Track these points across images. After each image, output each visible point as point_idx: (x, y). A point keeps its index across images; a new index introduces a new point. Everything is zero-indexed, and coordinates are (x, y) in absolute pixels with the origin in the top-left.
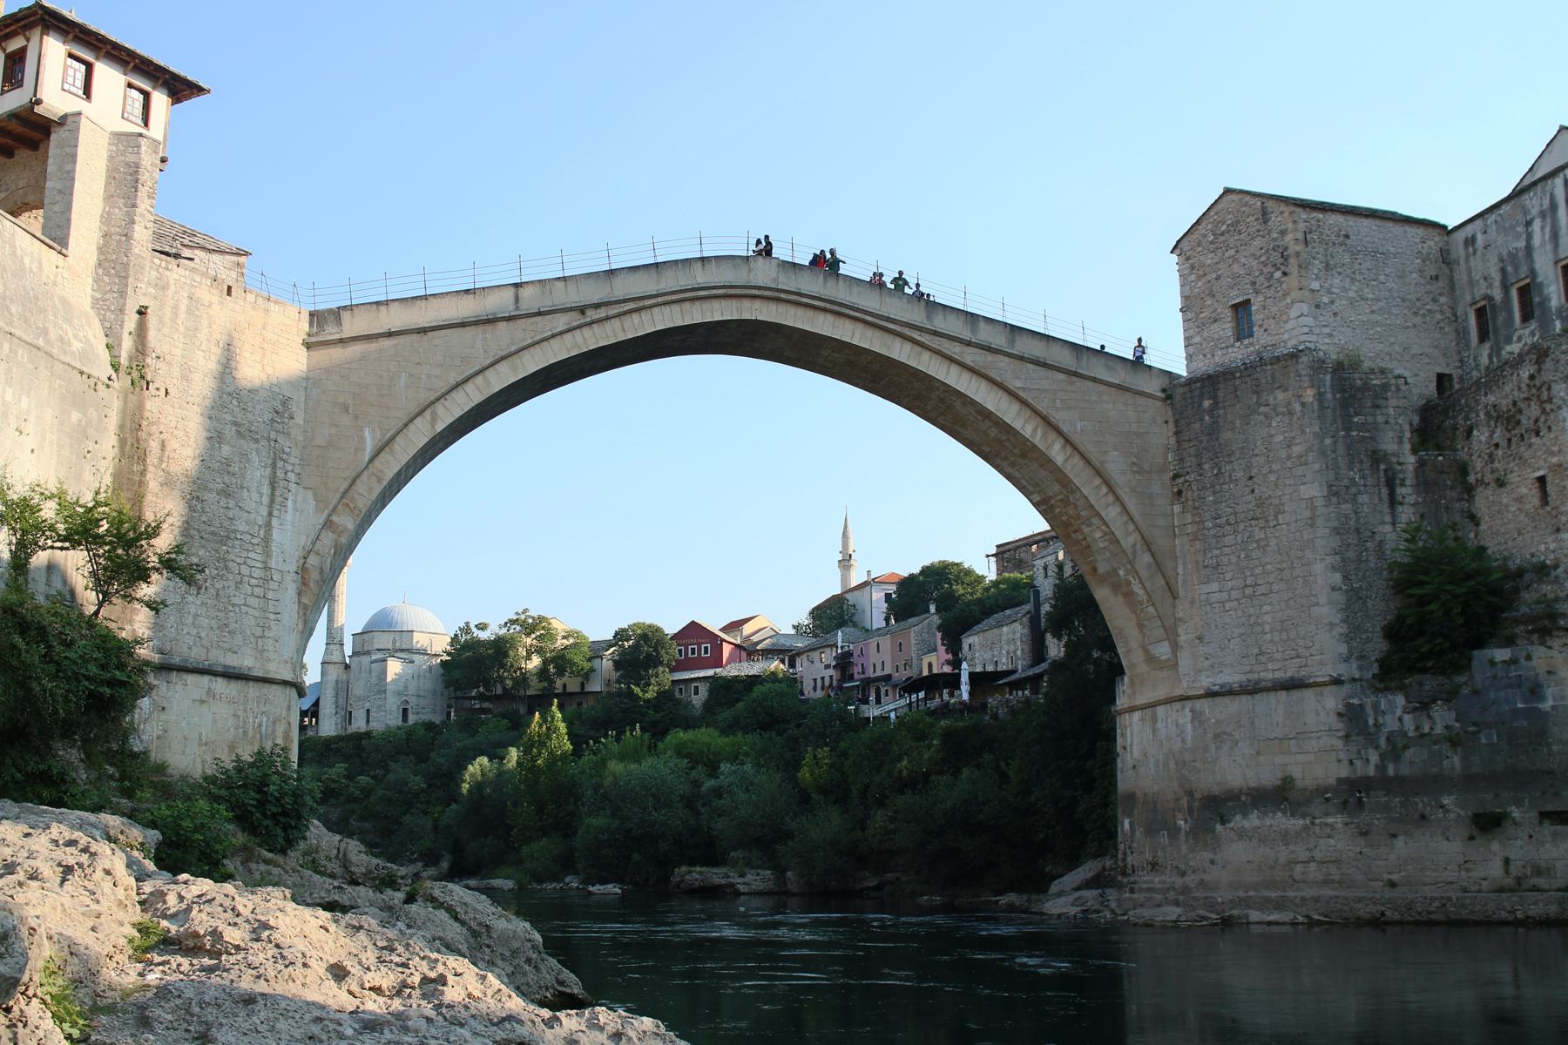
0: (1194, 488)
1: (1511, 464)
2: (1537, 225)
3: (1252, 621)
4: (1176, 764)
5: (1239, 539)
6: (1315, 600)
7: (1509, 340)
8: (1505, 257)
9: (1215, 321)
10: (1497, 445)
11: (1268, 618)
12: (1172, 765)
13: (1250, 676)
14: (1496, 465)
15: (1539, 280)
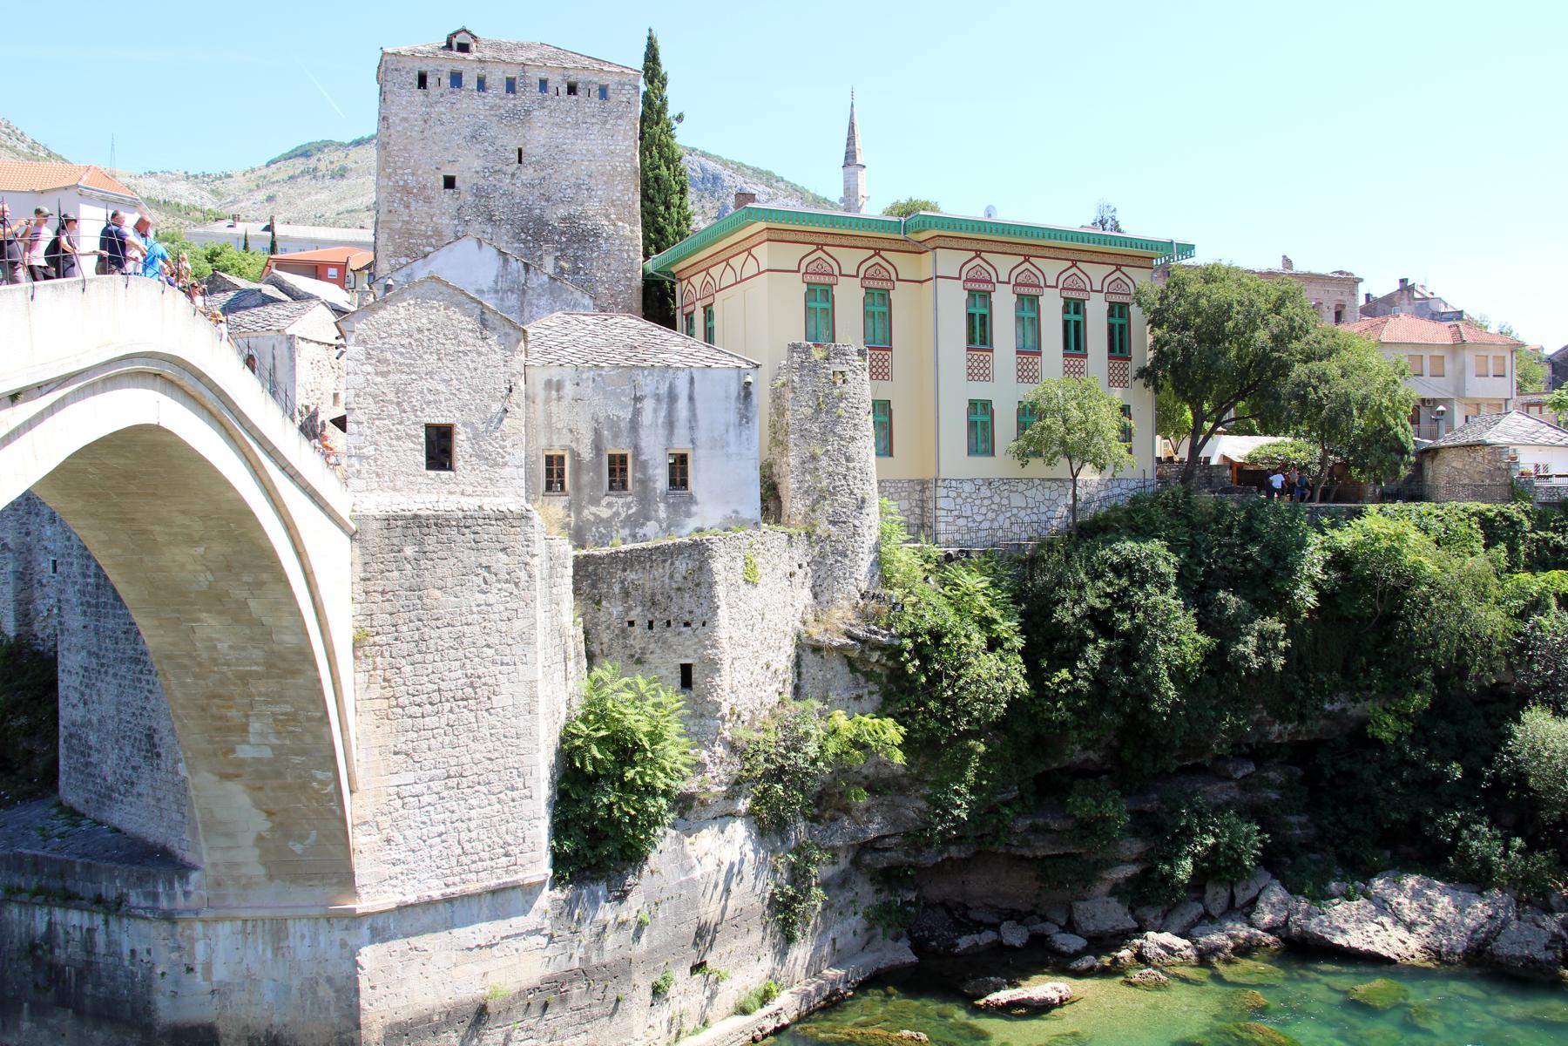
0: (387, 654)
1: (652, 646)
2: (648, 405)
3: (455, 817)
4: (337, 991)
5: (444, 721)
6: (528, 794)
7: (595, 501)
8: (601, 420)
9: (399, 438)
10: (631, 623)
11: (473, 813)
12: (326, 992)
13: (450, 880)
14: (630, 641)
15: (643, 458)
